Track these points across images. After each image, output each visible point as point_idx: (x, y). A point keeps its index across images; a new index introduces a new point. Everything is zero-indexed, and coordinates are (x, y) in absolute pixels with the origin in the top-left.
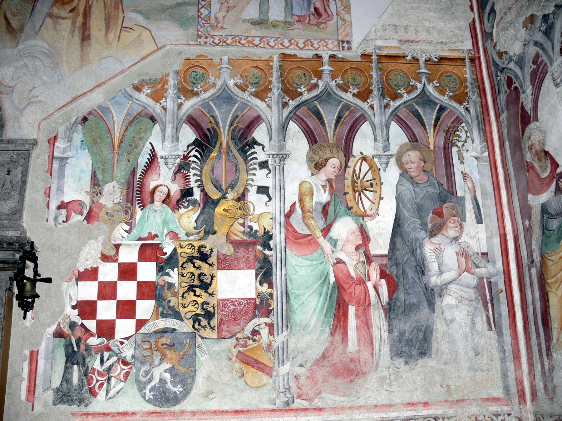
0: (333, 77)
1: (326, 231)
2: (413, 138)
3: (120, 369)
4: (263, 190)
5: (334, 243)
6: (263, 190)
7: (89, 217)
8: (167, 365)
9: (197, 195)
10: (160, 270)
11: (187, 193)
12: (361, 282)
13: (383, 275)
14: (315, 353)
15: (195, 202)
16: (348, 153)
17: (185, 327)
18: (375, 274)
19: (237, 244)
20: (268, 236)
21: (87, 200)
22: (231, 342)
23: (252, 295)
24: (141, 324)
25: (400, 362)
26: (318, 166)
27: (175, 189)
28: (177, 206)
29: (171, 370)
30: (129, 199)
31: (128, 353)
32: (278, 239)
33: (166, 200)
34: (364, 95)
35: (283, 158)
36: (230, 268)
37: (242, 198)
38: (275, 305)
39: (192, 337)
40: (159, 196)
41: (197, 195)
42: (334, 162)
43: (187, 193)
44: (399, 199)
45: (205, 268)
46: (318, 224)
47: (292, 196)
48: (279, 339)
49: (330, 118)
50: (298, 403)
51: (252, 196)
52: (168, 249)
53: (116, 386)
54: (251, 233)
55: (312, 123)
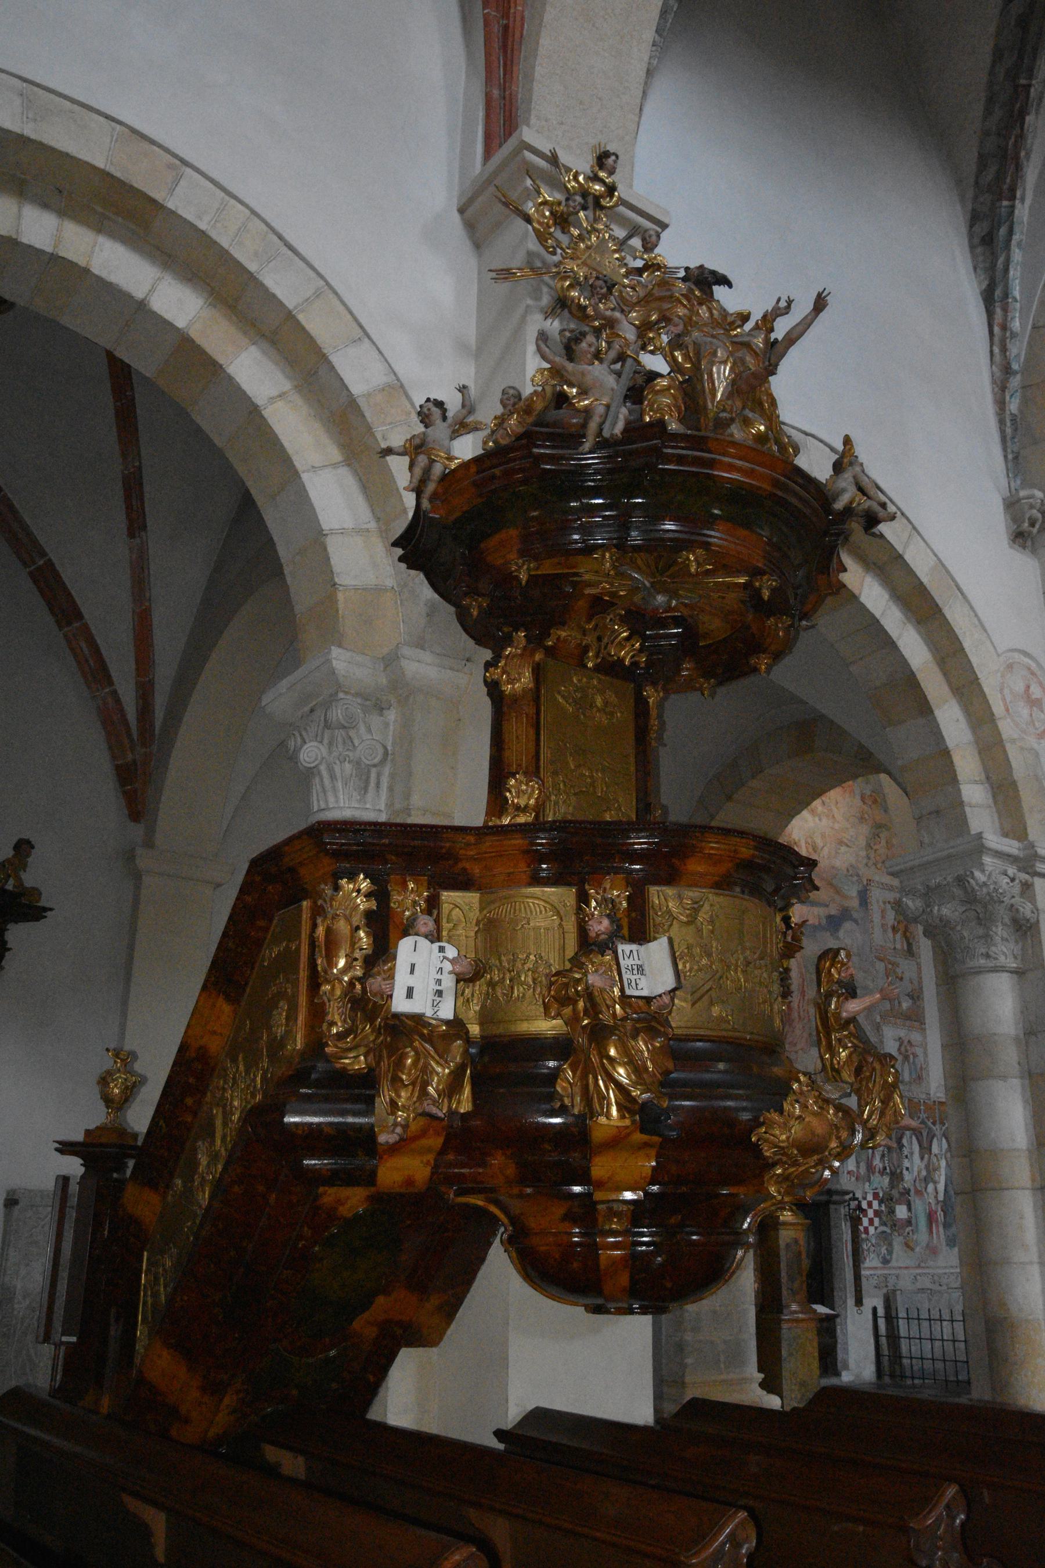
0: (925, 1113)
1: (926, 1189)
2: (949, 1145)
3: (872, 1249)
4: (907, 1169)
5: (928, 1194)
6: (907, 1169)
7: (857, 1179)
8: (885, 1247)
9: (888, 1171)
10: (880, 1205)
11: (885, 1168)
12: (936, 1213)
13: (942, 1210)
14: (924, 1244)
15: (887, 1173)
16: (931, 1154)
17: (889, 1231)
18: (940, 1210)
19: (902, 1194)
20: (909, 1190)
21: (855, 1170)
22: (901, 1238)
23: (906, 1217)
24: (876, 1228)
25: (948, 1248)
26: (922, 1158)
27: (881, 1166)
28: (882, 1175)
29: (887, 1249)
30: (868, 1171)
31: (874, 1241)
32: (912, 1193)
33: (879, 1172)
34: (934, 1123)
35: (912, 1153)
36: (900, 1204)
37: (901, 1173)
38: (913, 1221)
39: (891, 1234)
40: (877, 1170)
41: (888, 1171)
42: (926, 1156)
43: (885, 1168)
44: (946, 1175)
45: (892, 1204)
46: (923, 1185)
47: (916, 1173)
48: (915, 1237)
49: (925, 1134)
50: (923, 1265)
51: (905, 1172)
52: (881, 1195)
53: (872, 1256)
54: (904, 1188)
55: (920, 1138)
